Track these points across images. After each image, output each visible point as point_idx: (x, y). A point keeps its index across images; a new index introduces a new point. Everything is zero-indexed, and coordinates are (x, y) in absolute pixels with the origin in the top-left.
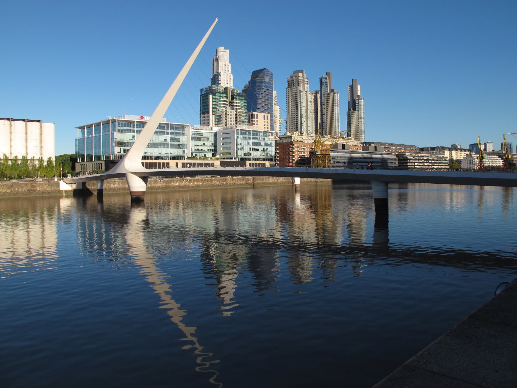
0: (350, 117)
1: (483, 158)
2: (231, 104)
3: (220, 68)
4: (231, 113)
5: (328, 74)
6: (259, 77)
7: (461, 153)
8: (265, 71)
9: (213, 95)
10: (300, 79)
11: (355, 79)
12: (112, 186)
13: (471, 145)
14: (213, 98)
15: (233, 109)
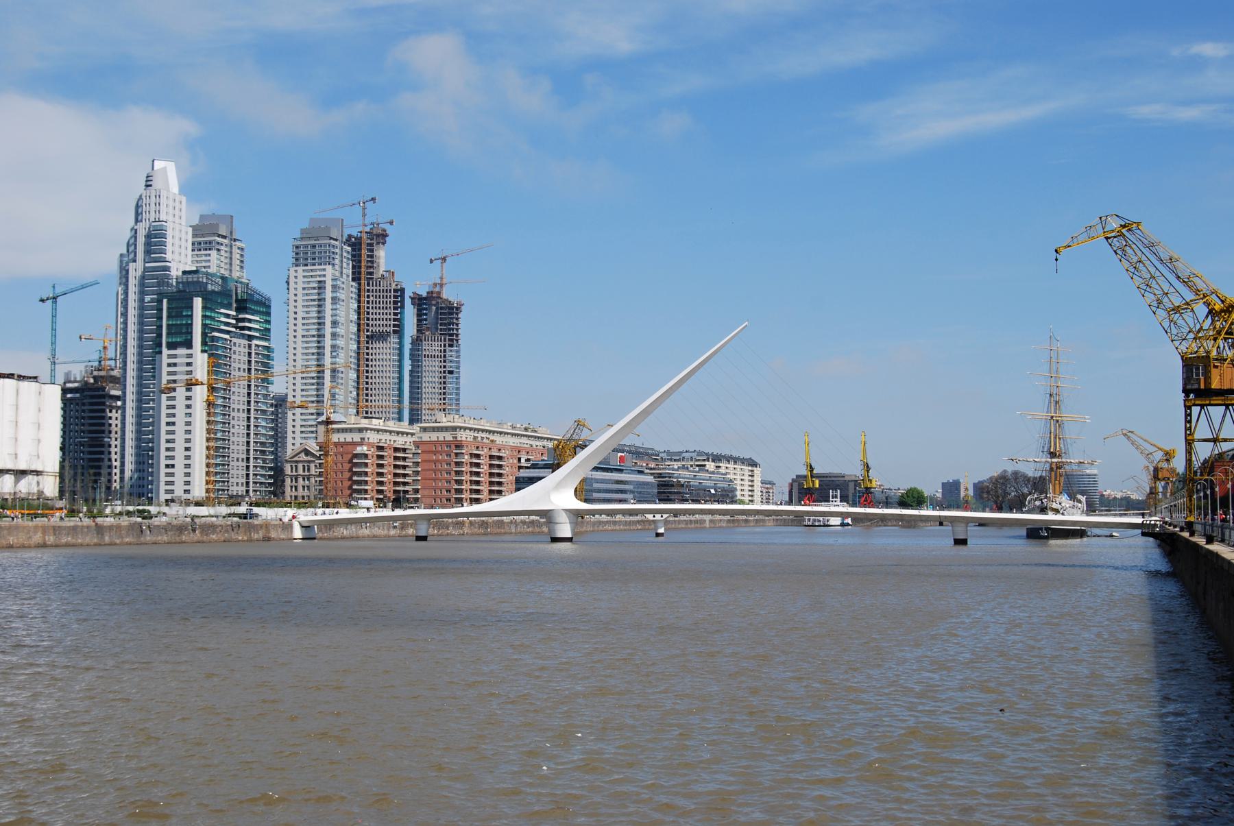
15: (243, 336)
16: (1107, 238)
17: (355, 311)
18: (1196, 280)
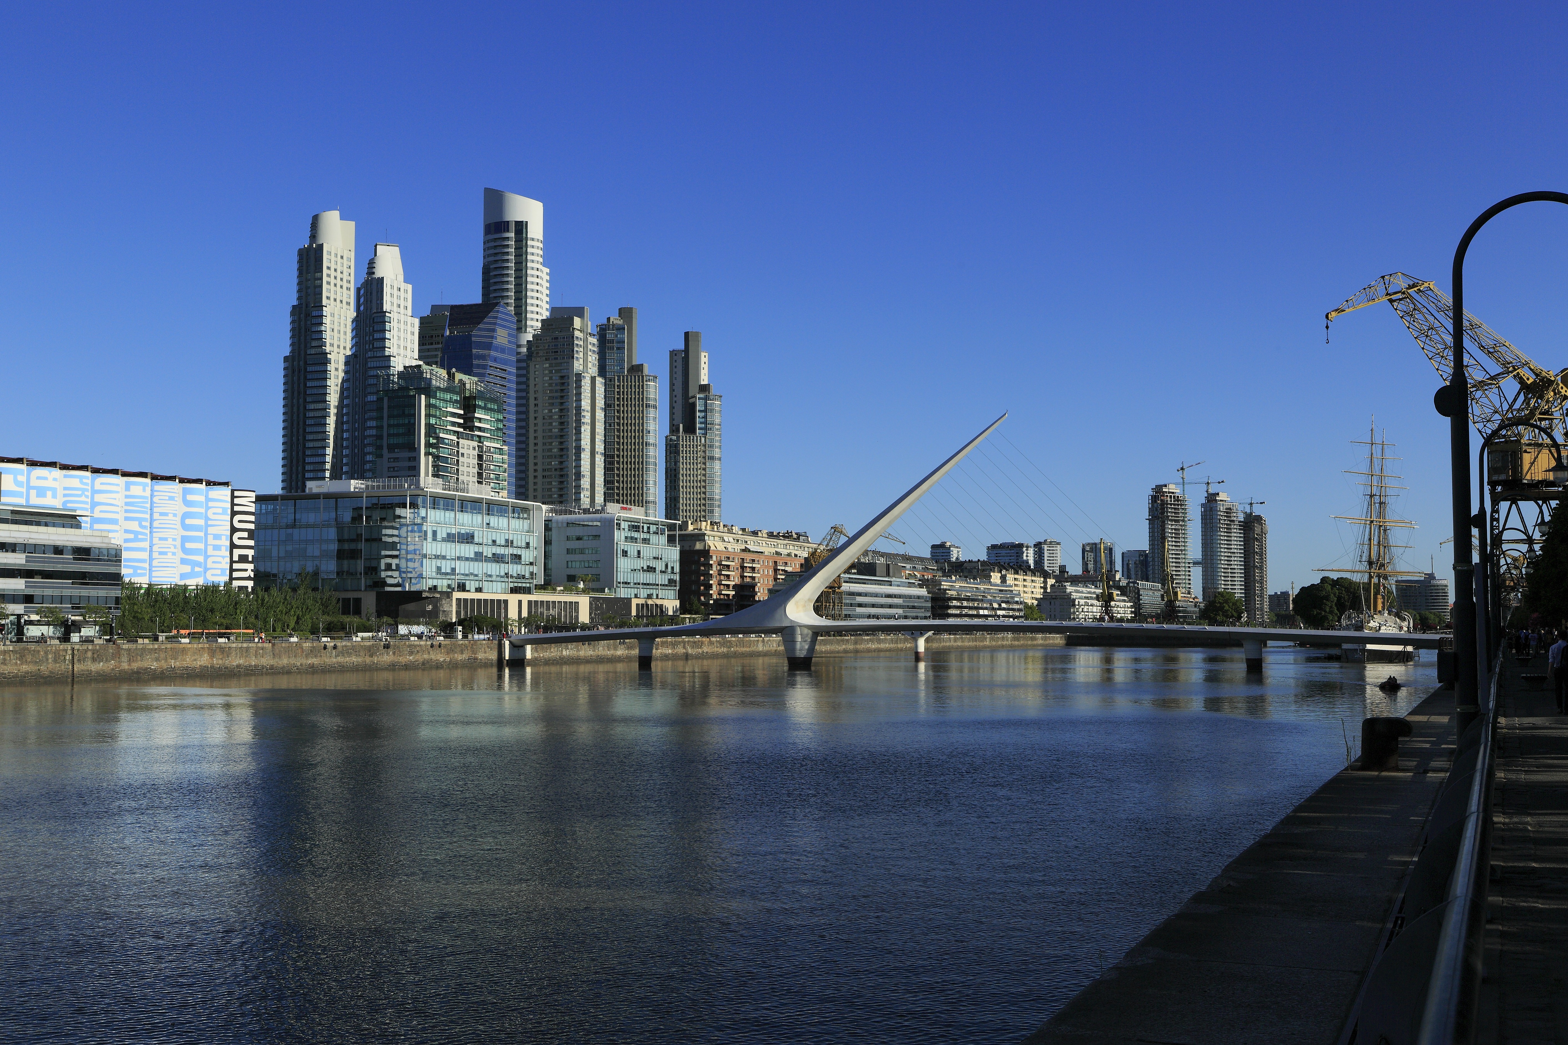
0: (677, 453)
1: (1110, 598)
2: (468, 423)
3: (387, 298)
4: (468, 448)
5: (626, 313)
6: (480, 329)
7: (1025, 580)
8: (498, 312)
9: (428, 396)
10: (577, 338)
11: (697, 334)
12: (564, 653)
13: (994, 547)
14: (429, 406)
15: (472, 438)
16: (1391, 301)
17: (602, 409)
18: (1502, 349)
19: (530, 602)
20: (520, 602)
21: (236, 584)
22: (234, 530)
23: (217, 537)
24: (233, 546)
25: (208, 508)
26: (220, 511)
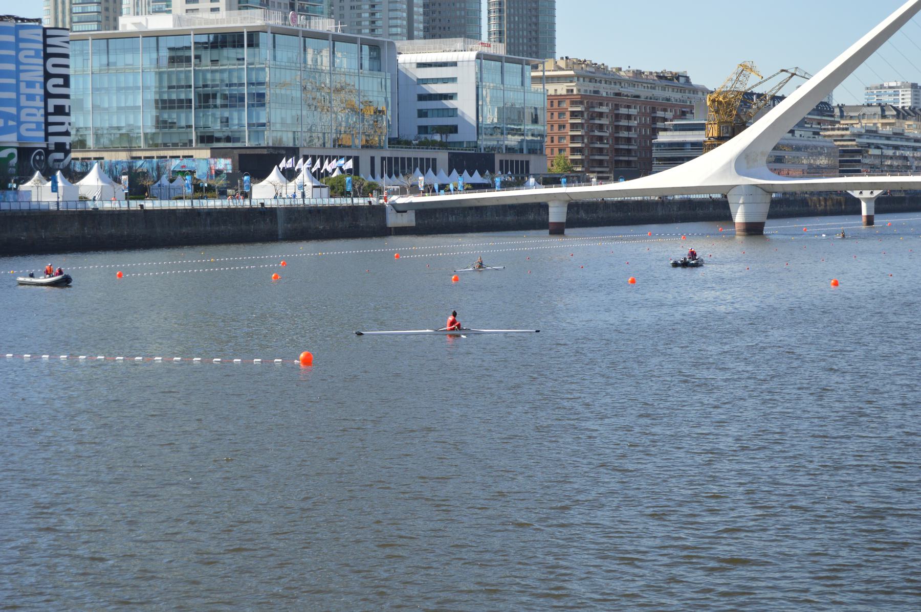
19: (383, 159)
20: (373, 159)
21: (53, 140)
22: (47, 76)
23: (30, 84)
24: (47, 95)
25: (18, 50)
26: (32, 53)
